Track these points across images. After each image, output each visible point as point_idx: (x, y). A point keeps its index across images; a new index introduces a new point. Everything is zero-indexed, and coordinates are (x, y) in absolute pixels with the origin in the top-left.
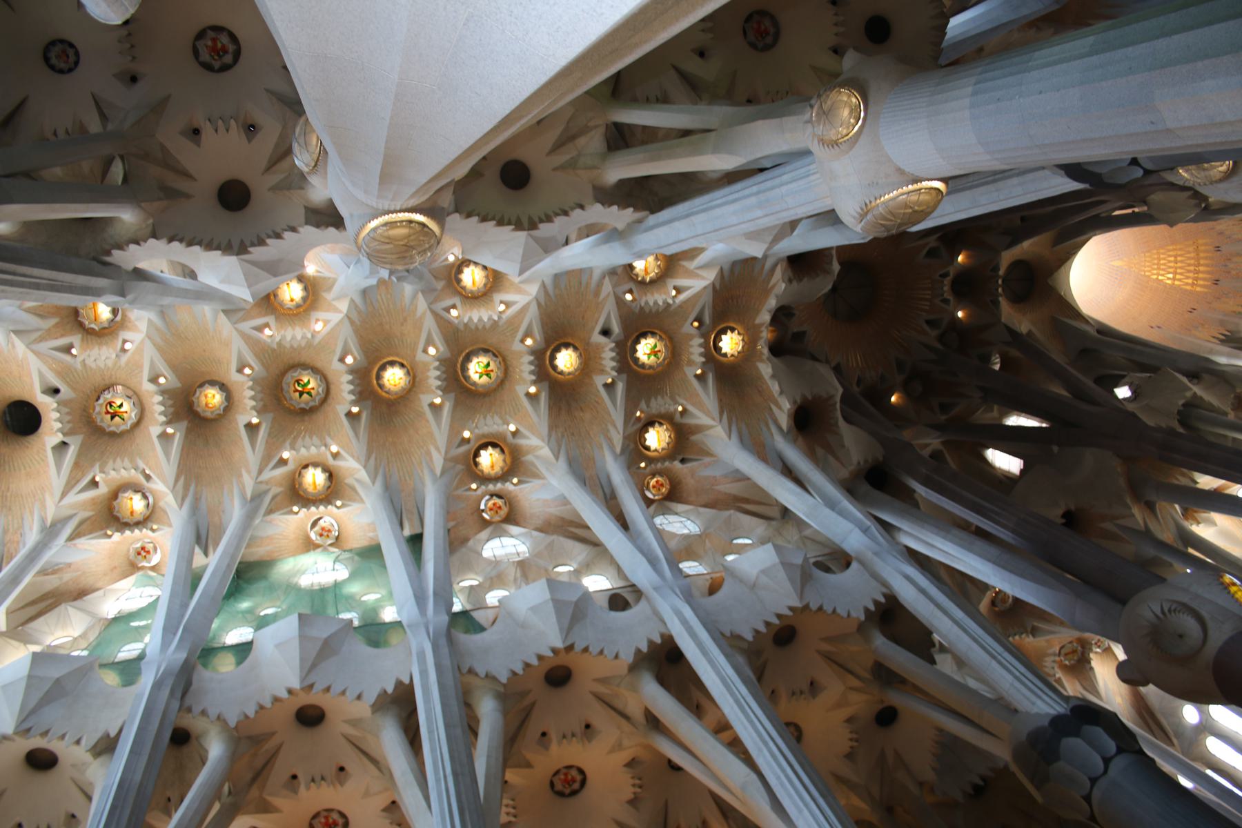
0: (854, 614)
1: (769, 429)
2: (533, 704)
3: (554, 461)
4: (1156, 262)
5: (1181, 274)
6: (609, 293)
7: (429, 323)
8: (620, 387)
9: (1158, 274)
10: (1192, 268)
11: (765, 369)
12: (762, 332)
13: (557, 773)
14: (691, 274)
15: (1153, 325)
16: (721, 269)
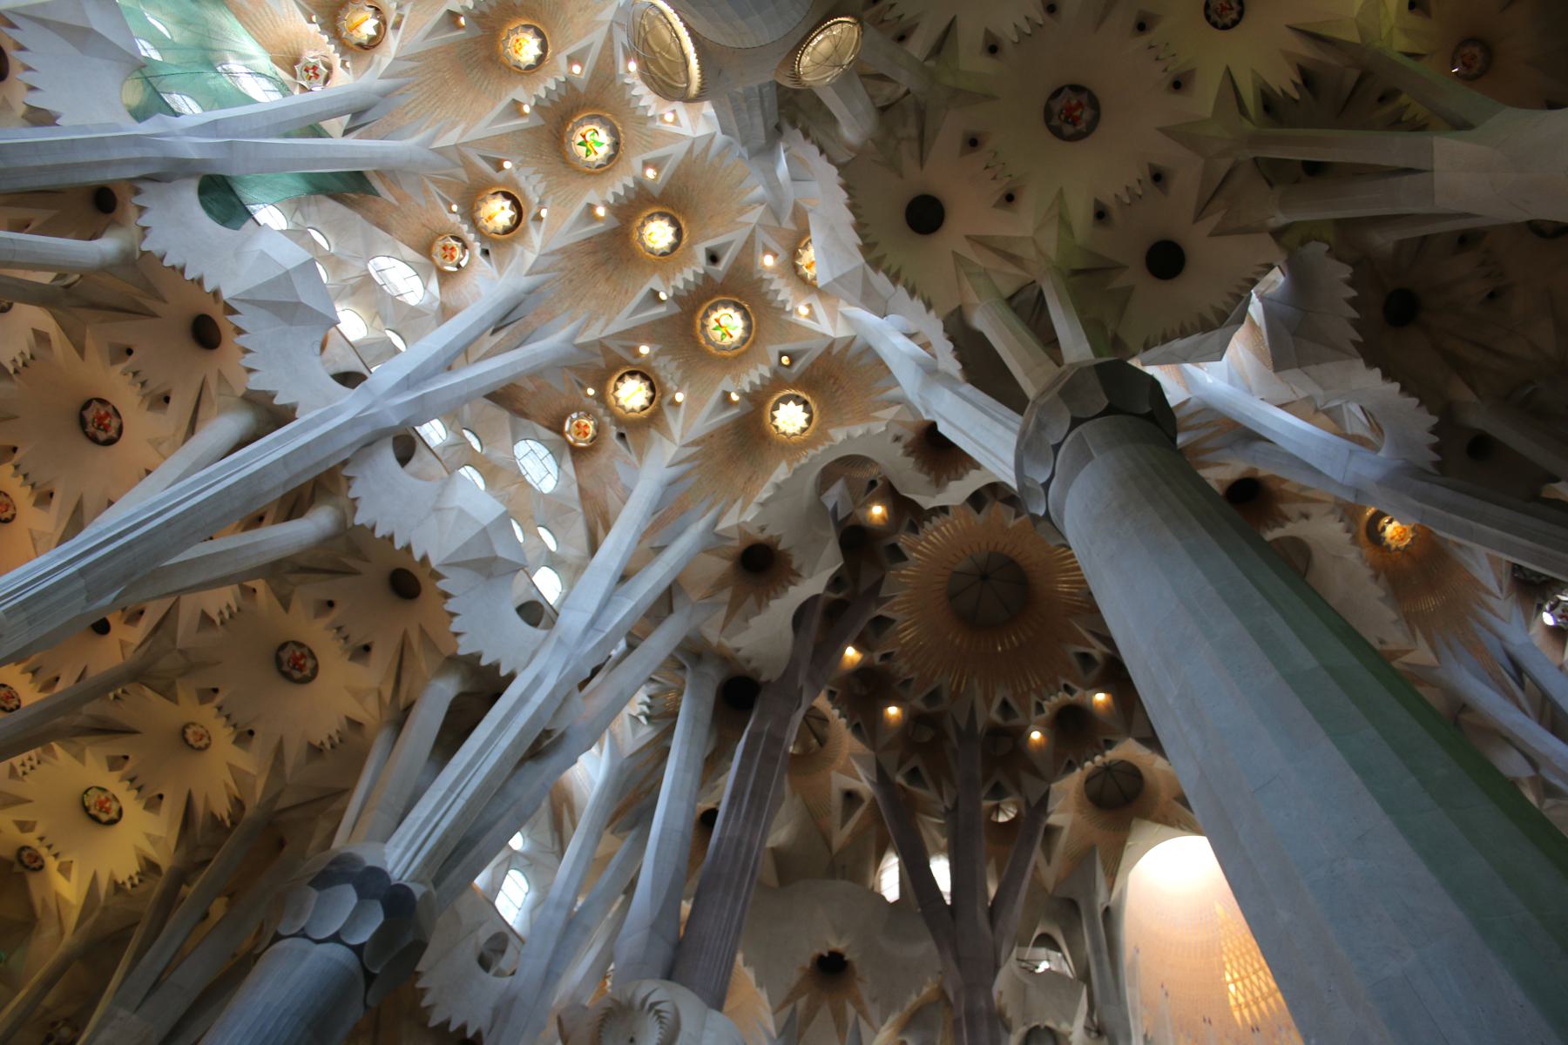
0: (461, 640)
1: (709, 509)
2: (153, 315)
3: (524, 272)
4: (1244, 950)
5: (1244, 986)
6: (751, 223)
7: (597, 37)
8: (661, 310)
9: (1230, 961)
10: (1257, 994)
11: (781, 472)
12: (823, 445)
13: (103, 402)
14: (832, 314)
15: (1166, 986)
16: (854, 338)
